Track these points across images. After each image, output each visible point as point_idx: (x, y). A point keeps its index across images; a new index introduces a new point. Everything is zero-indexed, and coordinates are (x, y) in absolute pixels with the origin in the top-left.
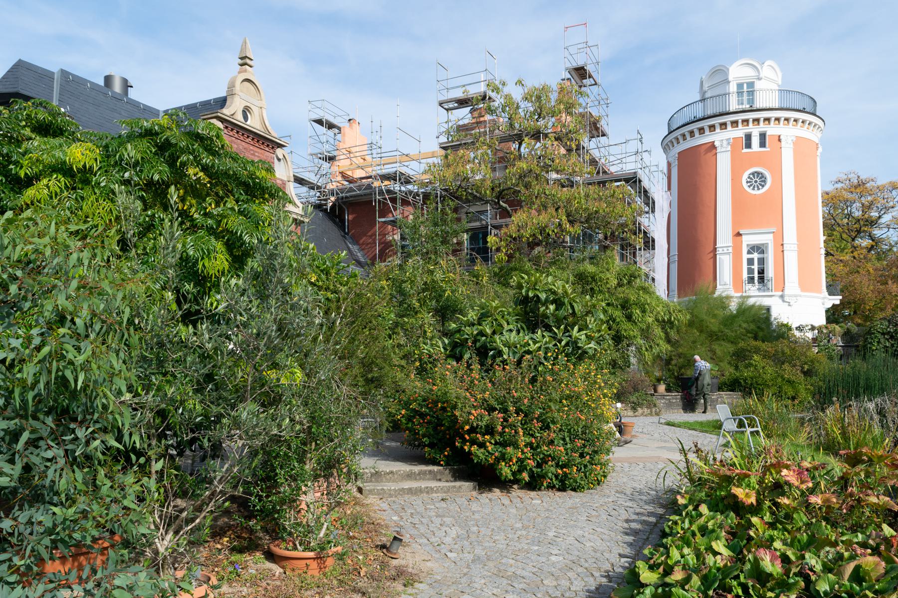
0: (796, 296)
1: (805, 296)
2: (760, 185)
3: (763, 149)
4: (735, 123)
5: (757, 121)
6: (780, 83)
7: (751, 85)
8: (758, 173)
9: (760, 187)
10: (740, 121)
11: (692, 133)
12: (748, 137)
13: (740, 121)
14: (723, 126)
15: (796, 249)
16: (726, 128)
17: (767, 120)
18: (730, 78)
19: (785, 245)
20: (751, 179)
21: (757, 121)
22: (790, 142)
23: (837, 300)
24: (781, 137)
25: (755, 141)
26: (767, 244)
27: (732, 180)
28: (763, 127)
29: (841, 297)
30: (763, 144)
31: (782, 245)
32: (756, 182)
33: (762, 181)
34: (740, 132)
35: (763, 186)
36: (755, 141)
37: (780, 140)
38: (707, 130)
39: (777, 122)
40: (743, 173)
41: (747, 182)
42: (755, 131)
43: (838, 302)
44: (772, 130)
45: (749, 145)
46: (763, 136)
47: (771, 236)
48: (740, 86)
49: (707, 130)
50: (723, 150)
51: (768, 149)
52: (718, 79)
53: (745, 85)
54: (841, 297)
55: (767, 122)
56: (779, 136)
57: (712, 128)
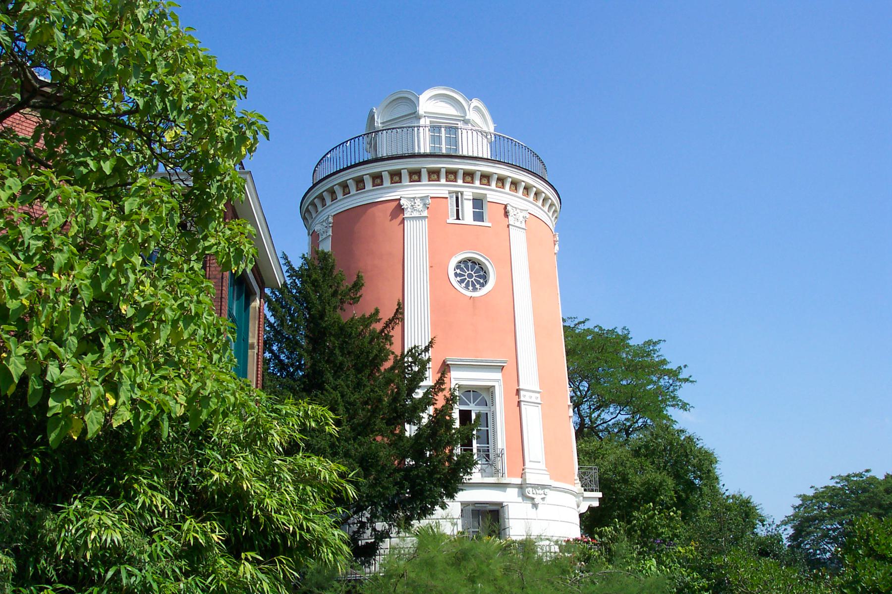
0: (543, 487)
1: (556, 489)
2: (478, 282)
4: (434, 174)
5: (469, 176)
8: (474, 262)
9: (478, 286)
10: (443, 171)
11: (360, 182)
13: (443, 172)
14: (416, 175)
17: (486, 178)
18: (422, 110)
19: (522, 393)
20: (462, 269)
21: (469, 176)
23: (594, 498)
24: (509, 208)
25: (468, 208)
26: (494, 386)
29: (600, 495)
30: (478, 217)
31: (518, 391)
32: (470, 276)
33: (480, 277)
34: (441, 189)
35: (482, 285)
37: (506, 214)
38: (386, 177)
39: (500, 184)
40: (450, 258)
41: (456, 275)
42: (468, 193)
43: (596, 504)
44: (494, 195)
46: (478, 202)
47: (498, 375)
48: (435, 128)
49: (386, 177)
50: (416, 214)
51: (490, 225)
52: (402, 110)
53: (443, 129)
54: (600, 495)
55: (485, 181)
56: (506, 206)
57: (396, 176)
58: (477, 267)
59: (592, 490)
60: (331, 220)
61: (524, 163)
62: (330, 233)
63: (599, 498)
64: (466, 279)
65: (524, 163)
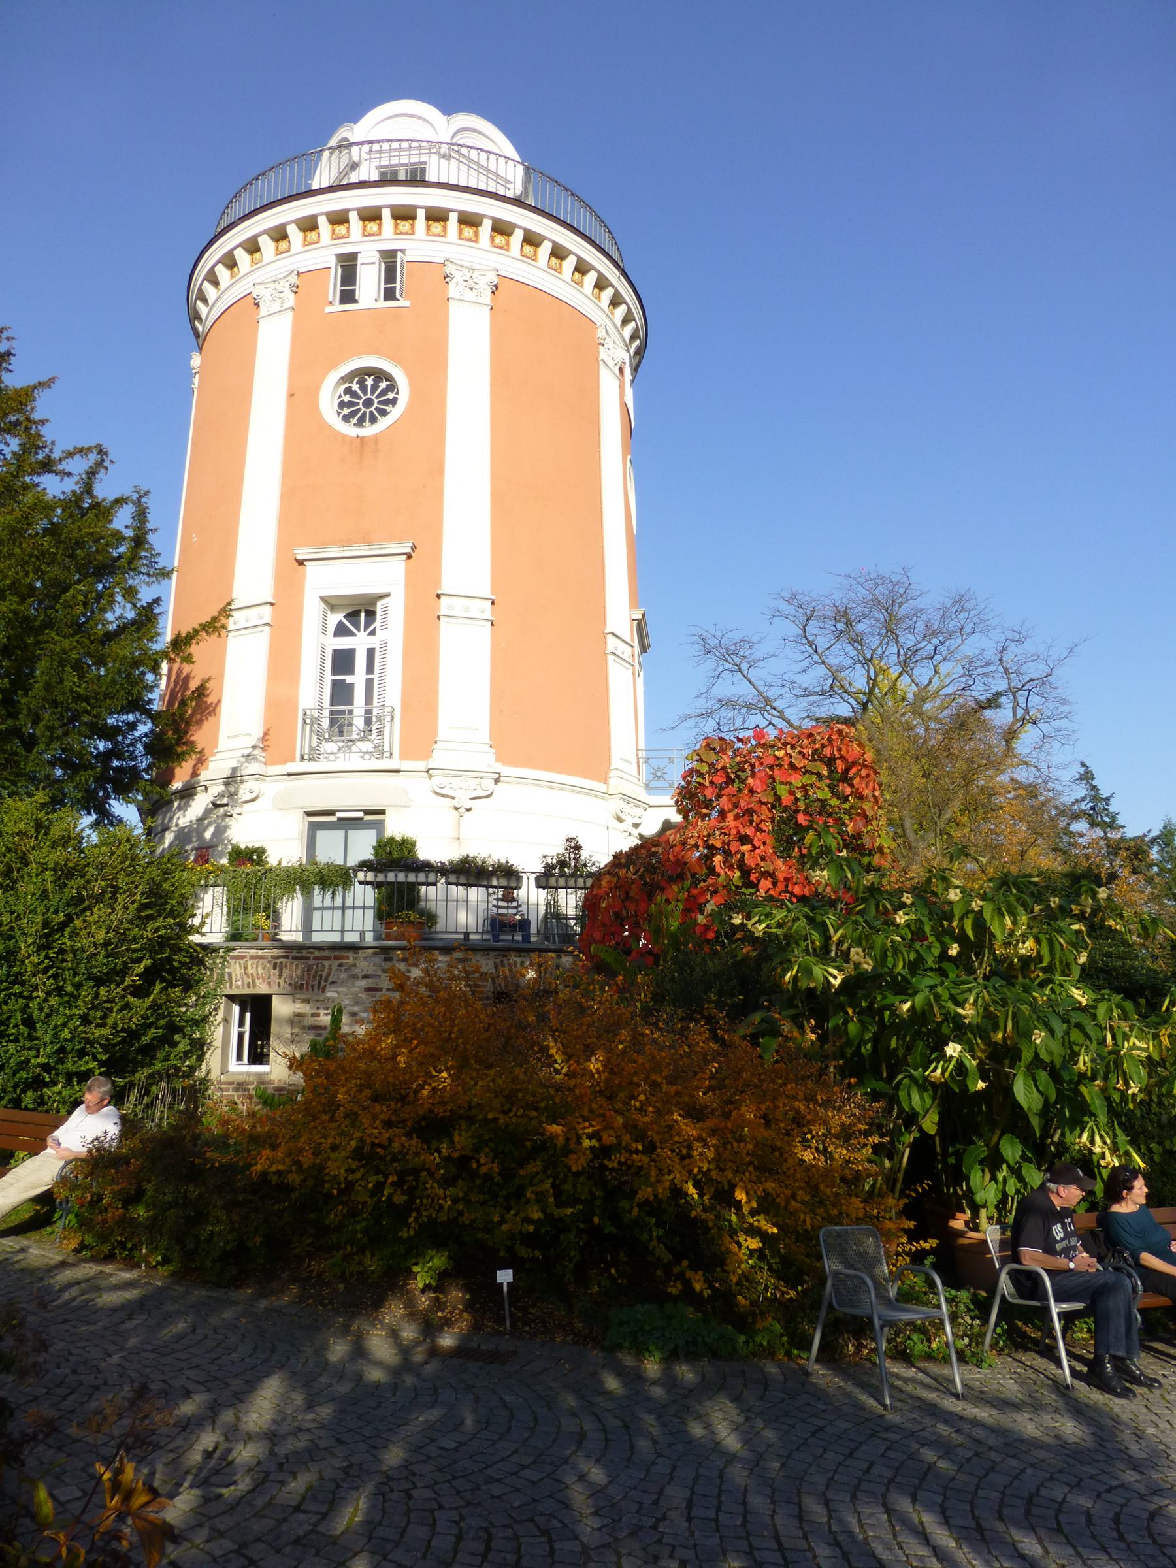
0: (477, 774)
8: (379, 375)
12: (348, 266)
17: (404, 214)
25: (369, 280)
32: (368, 403)
36: (369, 280)
45: (348, 297)
51: (406, 303)
58: (383, 385)
61: (579, 219)
64: (365, 413)
65: (579, 219)
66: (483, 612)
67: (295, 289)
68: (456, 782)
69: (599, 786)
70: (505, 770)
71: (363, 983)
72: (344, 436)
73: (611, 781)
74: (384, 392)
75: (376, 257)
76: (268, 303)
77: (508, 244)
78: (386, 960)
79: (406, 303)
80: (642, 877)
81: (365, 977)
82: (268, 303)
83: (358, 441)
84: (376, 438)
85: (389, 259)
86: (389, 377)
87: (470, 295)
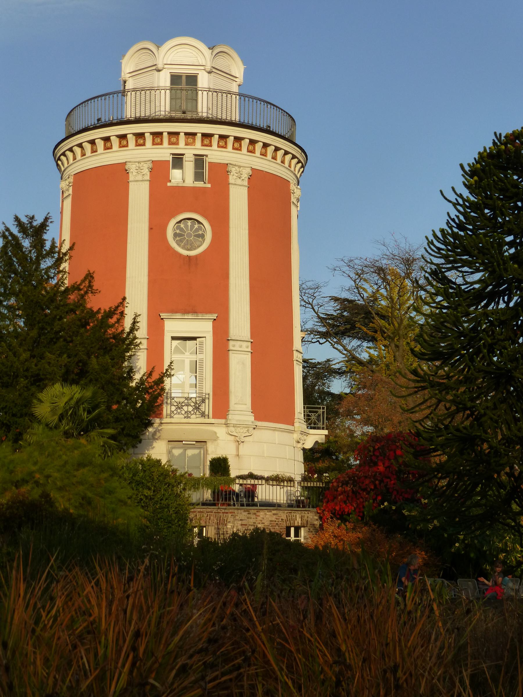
0: (247, 427)
3: (200, 184)
6: (240, 79)
7: (192, 79)
15: (249, 349)
16: (144, 145)
22: (245, 176)
24: (230, 168)
27: (151, 229)
28: (198, 148)
29: (326, 432)
41: (175, 235)
48: (175, 79)
50: (140, 178)
51: (209, 186)
54: (326, 432)
59: (319, 428)
60: (71, 180)
62: (70, 192)
63: (326, 435)
66: (247, 347)
67: (152, 170)
68: (238, 430)
69: (290, 427)
70: (259, 423)
71: (240, 522)
72: (180, 255)
73: (295, 424)
74: (197, 230)
75: (193, 158)
76: (134, 174)
77: (254, 149)
78: (248, 514)
79: (209, 186)
80: (352, 489)
81: (241, 520)
82: (134, 174)
83: (188, 258)
84: (196, 257)
85: (199, 160)
86: (199, 222)
87: (239, 182)
